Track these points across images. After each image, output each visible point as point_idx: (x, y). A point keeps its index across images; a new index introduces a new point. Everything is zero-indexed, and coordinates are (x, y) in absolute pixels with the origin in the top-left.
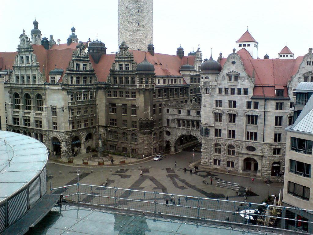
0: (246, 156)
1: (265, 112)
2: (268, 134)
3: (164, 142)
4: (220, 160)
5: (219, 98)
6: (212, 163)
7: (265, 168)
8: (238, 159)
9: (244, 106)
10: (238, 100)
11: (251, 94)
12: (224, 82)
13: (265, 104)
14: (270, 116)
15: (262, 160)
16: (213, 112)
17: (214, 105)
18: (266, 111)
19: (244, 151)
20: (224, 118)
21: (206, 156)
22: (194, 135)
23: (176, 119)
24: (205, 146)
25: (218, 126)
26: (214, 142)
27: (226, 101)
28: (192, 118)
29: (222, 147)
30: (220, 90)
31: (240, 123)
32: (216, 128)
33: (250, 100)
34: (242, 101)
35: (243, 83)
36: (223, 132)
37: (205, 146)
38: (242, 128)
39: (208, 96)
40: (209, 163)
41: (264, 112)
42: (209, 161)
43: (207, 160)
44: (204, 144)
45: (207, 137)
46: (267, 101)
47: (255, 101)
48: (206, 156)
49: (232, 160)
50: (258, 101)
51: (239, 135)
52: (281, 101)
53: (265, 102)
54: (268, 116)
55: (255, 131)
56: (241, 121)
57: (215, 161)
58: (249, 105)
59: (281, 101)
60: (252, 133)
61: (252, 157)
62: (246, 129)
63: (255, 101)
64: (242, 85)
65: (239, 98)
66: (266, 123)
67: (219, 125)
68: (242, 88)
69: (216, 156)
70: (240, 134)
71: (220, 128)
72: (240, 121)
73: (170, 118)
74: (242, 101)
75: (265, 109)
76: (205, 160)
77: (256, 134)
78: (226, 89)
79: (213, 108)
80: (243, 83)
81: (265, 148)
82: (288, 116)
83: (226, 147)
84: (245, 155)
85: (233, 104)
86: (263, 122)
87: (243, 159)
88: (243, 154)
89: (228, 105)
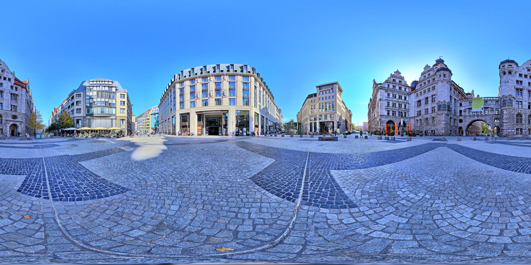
21: (509, 127)
40: (512, 133)
42: (512, 131)
43: (510, 131)
48: (509, 127)
57: (517, 129)
76: (508, 131)
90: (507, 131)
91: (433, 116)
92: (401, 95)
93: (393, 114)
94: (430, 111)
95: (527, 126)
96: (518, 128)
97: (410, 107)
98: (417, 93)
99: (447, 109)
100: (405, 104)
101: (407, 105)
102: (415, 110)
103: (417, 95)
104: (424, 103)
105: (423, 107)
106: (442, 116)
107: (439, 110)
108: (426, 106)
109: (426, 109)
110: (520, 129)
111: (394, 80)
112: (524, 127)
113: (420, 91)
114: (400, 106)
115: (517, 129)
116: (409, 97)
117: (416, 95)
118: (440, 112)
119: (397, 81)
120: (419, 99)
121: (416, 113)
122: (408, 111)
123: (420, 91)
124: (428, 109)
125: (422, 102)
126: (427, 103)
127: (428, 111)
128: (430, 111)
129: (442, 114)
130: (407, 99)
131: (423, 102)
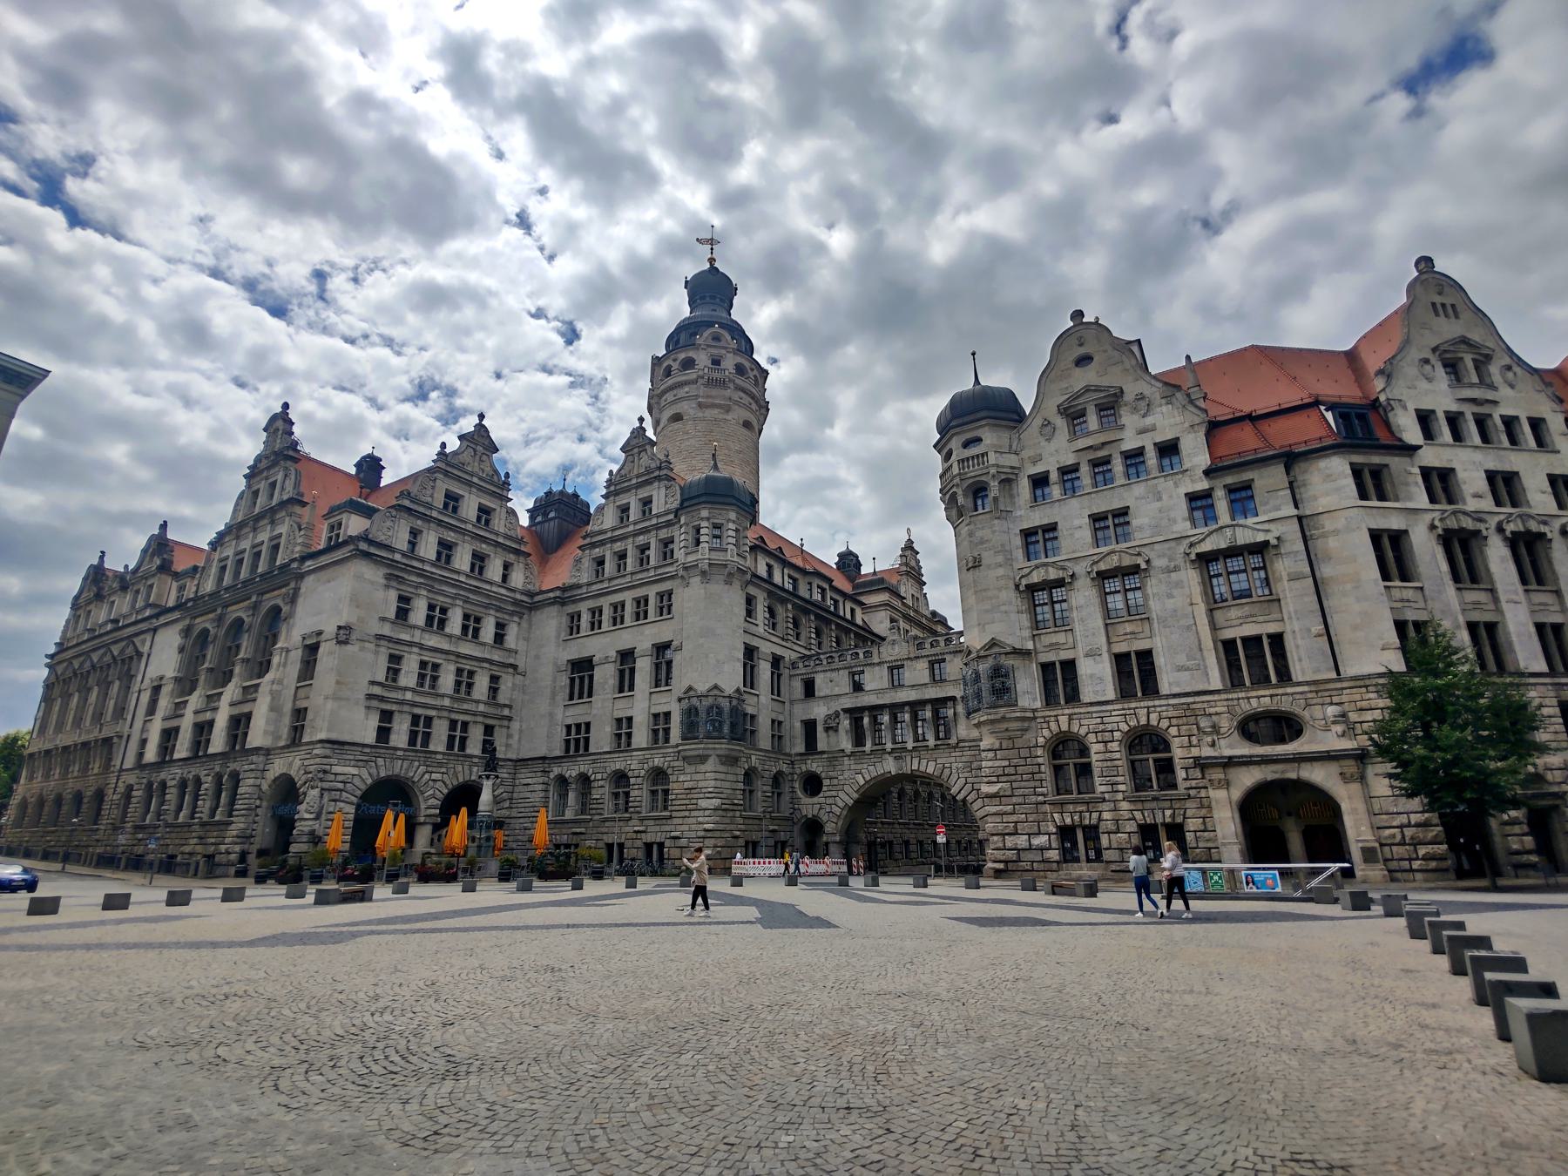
0: (1248, 778)
1: (1300, 519)
2: (1355, 628)
3: (796, 829)
4: (1096, 827)
5: (1037, 518)
6: (1054, 855)
7: (1401, 827)
8: (1206, 805)
9: (1175, 521)
10: (1137, 498)
11: (1196, 455)
12: (1053, 446)
13: (1291, 483)
14: (1336, 532)
15: (1362, 778)
16: (1017, 586)
17: (1019, 554)
18: (1308, 513)
19: (1230, 746)
20: (1082, 602)
21: (1014, 818)
22: (930, 770)
23: (844, 710)
24: (997, 763)
25: (1054, 646)
26: (1046, 733)
27: (1077, 522)
28: (911, 695)
29: (1095, 748)
30: (1040, 481)
31: (1170, 604)
32: (1046, 658)
33: (1203, 485)
34: (1160, 499)
35: (1149, 421)
36: (1085, 668)
37: (997, 763)
38: (1188, 628)
39: (988, 516)
41: (1296, 520)
42: (1037, 841)
43: (1022, 841)
44: (991, 755)
45: (1002, 710)
46: (1298, 469)
47: (1230, 480)
48: (1014, 818)
49: (1168, 813)
50: (1246, 476)
51: (1181, 669)
52: (1376, 459)
53: (1288, 473)
54: (1324, 536)
55: (1273, 628)
56: (1175, 592)
57: (1066, 833)
58: (1199, 502)
59: (1376, 459)
60: (1253, 642)
61: (1293, 775)
62: (1214, 627)
63: (1230, 480)
64: (1142, 431)
65: (1139, 489)
66: (1325, 571)
67: (1061, 638)
68: (1148, 443)
69: (1071, 807)
70: (1182, 659)
71: (1065, 655)
72: (1170, 596)
73: (819, 711)
74: (1160, 499)
75: (1297, 507)
76: (1010, 841)
77: (1277, 640)
78: (1068, 472)
79: (1017, 566)
80: (1149, 421)
81: (1364, 704)
82: (1433, 527)
83: (1114, 746)
84: (1244, 769)
85: (1113, 522)
86: (1308, 569)
87: (1237, 794)
88: (1230, 763)
89: (1086, 534)
90: (1009, 845)
91: (657, 762)
92: (478, 611)
93: (413, 736)
94: (641, 737)
95: (1125, 805)
96: (1068, 821)
97: (523, 689)
98: (571, 609)
99: (726, 729)
100: (496, 671)
101: (507, 682)
102: (551, 715)
103: (575, 618)
104: (613, 682)
105: (602, 709)
106: (702, 768)
107: (690, 731)
108: (620, 704)
109: (619, 720)
110: (1084, 828)
111: (452, 500)
112: (1106, 815)
113: (591, 604)
114: (464, 682)
115: (1066, 833)
116: (524, 624)
117: (565, 620)
118: (693, 748)
119: (469, 508)
120: (586, 654)
121: (561, 734)
122: (510, 719)
123: (591, 604)
124: (630, 719)
125: (598, 673)
126: (626, 682)
127: (629, 735)
128: (641, 737)
129: (703, 759)
130: (511, 640)
131: (605, 676)
